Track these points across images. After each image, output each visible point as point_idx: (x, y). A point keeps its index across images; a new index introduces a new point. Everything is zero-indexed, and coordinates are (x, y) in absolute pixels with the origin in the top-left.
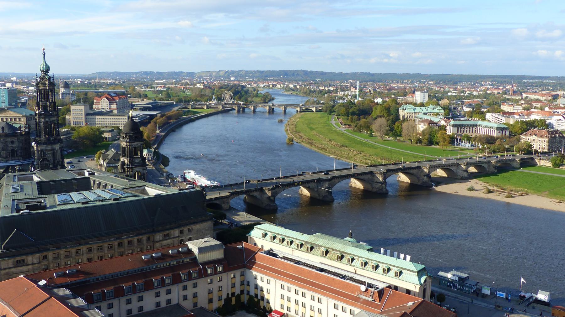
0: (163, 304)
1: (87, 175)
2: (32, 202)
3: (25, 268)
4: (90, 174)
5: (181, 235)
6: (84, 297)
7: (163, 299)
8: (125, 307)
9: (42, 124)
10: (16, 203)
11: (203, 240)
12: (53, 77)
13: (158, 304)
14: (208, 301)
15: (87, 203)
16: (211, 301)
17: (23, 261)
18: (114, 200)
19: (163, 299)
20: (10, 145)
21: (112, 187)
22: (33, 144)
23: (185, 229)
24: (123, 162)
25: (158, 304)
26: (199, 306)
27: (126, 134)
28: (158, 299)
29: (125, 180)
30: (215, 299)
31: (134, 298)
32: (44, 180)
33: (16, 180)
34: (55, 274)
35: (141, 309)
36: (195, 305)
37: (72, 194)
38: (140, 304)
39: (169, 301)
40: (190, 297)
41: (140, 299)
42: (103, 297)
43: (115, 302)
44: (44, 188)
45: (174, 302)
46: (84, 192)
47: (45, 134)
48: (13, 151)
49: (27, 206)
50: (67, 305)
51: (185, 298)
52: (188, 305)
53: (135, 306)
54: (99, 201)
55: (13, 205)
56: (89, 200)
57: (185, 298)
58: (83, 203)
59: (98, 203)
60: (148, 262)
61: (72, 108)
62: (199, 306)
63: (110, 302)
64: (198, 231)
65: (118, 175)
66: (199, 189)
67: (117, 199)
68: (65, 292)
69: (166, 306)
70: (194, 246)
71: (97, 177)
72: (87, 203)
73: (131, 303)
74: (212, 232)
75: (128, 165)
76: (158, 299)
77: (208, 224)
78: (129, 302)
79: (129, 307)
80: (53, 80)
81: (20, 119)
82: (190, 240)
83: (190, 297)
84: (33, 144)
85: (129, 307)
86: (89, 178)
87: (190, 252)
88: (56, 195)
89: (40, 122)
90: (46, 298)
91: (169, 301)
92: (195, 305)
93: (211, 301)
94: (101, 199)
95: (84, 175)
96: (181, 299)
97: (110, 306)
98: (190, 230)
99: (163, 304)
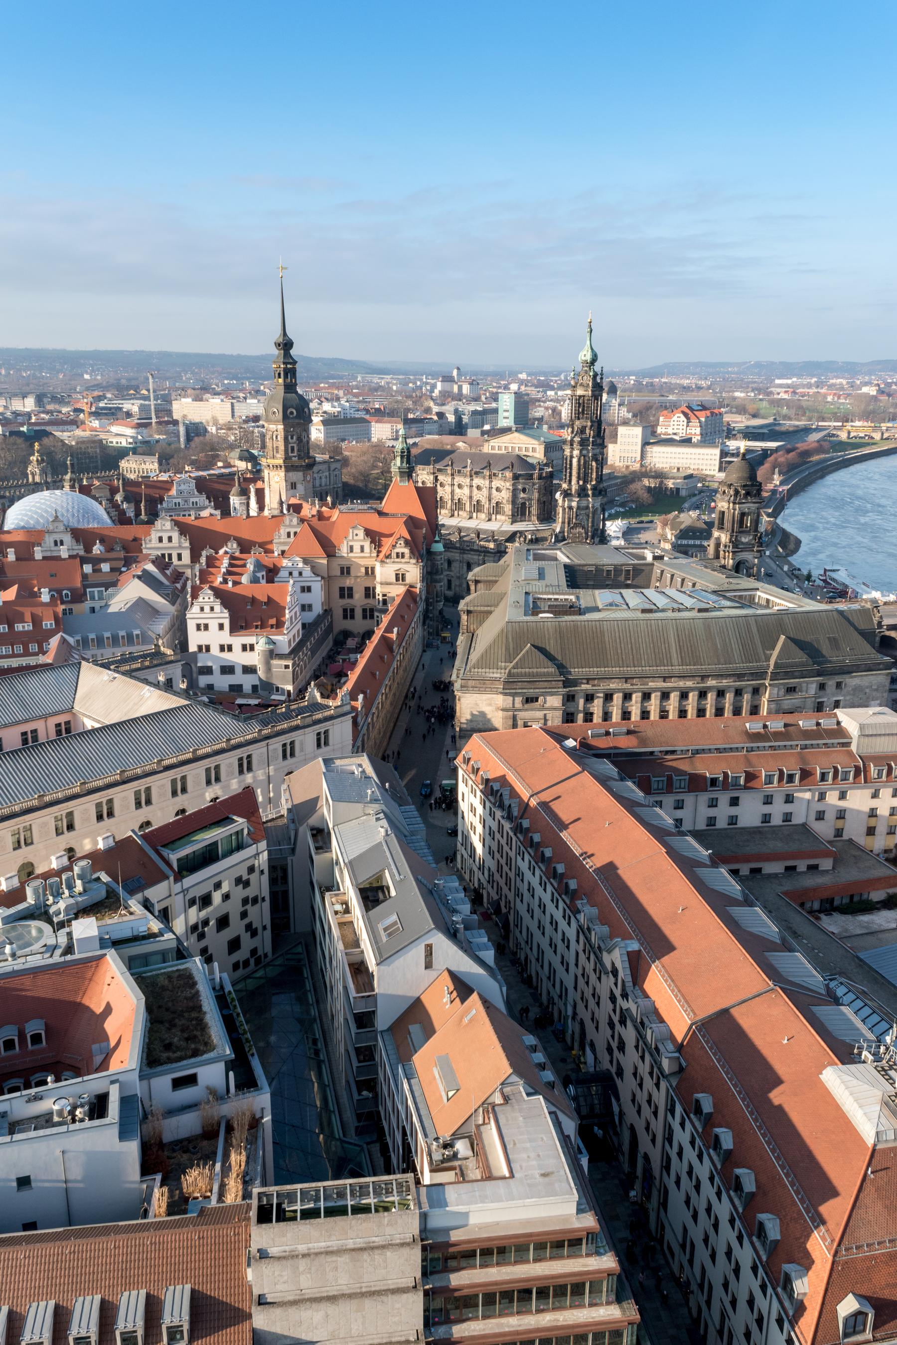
0: (777, 821)
1: (649, 557)
2: (556, 600)
3: (539, 714)
4: (655, 558)
5: (822, 693)
6: (636, 780)
7: (777, 810)
8: (705, 812)
9: (575, 461)
10: (531, 600)
11: (870, 711)
12: (602, 374)
13: (766, 818)
14: (865, 830)
15: (650, 611)
16: (871, 831)
17: (537, 701)
18: (700, 610)
19: (777, 810)
20: (522, 495)
21: (694, 585)
22: (558, 494)
23: (831, 683)
24: (718, 539)
25: (766, 818)
26: (845, 837)
27: (730, 486)
28: (767, 809)
29: (720, 575)
30: (881, 829)
31: (724, 798)
32: (577, 562)
33: (531, 558)
34: (590, 732)
35: (733, 820)
36: (839, 833)
37: (623, 591)
38: (734, 811)
39: (787, 817)
40: (830, 816)
41: (734, 802)
42: (669, 788)
43: (689, 799)
44: (575, 577)
45: (797, 820)
46: (645, 591)
47: (579, 478)
48: (524, 504)
49: (549, 606)
50: (609, 790)
51: (820, 816)
52: (825, 830)
53: (723, 812)
54: (673, 610)
55: (526, 601)
56: (654, 607)
57: (820, 816)
58: (644, 611)
59: (670, 614)
60: (755, 737)
61: (622, 430)
62: (845, 837)
63: (680, 797)
64: (858, 689)
65: (707, 563)
66: (868, 606)
67: (706, 610)
68: (608, 768)
69: (781, 823)
70: (850, 720)
71: (666, 564)
72: (650, 611)
73: (716, 806)
74: (886, 695)
75: (725, 546)
76: (767, 809)
77: (880, 678)
78: (713, 804)
79: (712, 812)
80: (602, 379)
81: (534, 450)
82: (837, 705)
83: (830, 816)
84: (558, 495)
85: (712, 812)
86: (653, 565)
87: (839, 732)
88: (597, 592)
89: (572, 457)
90: (576, 771)
91: (787, 817)
92: (839, 833)
93: (871, 831)
94: (676, 606)
95: (644, 558)
96: (813, 816)
97: (679, 806)
98: (839, 685)
99: (777, 821)
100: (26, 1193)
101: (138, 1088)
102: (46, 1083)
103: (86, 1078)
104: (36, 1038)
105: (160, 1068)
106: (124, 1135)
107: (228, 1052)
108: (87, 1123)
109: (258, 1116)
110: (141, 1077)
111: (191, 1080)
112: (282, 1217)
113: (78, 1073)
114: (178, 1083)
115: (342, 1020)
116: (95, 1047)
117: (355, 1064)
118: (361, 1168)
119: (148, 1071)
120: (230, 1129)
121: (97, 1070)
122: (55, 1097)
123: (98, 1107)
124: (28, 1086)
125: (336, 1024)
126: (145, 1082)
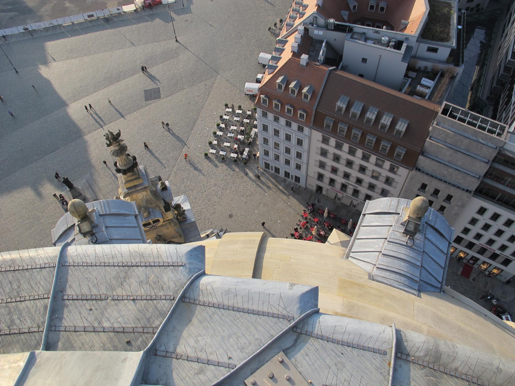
100: (363, 64)
101: (413, 42)
102: (382, 28)
103: (397, 32)
104: (382, 9)
105: (425, 40)
106: (404, 59)
107: (454, 45)
108: (392, 50)
109: (455, 75)
110: (417, 41)
111: (435, 50)
112: (451, 116)
113: (392, 28)
114: (430, 50)
115: (505, 51)
116: (403, 21)
117: (501, 72)
118: (482, 110)
119: (421, 40)
120: (442, 75)
121: (400, 31)
122: (385, 34)
123: (398, 45)
124: (373, 26)
125: (500, 51)
126: (418, 43)
